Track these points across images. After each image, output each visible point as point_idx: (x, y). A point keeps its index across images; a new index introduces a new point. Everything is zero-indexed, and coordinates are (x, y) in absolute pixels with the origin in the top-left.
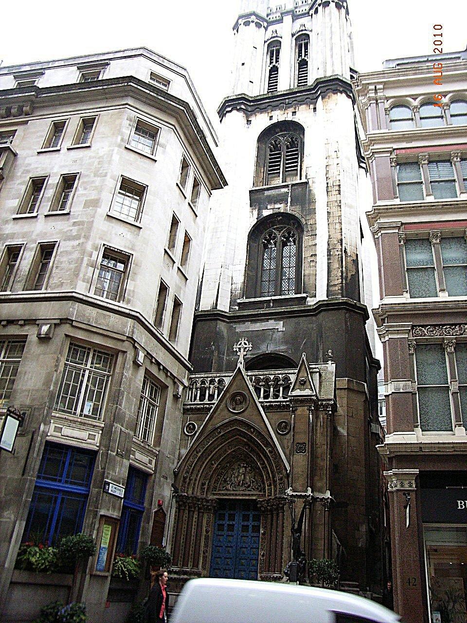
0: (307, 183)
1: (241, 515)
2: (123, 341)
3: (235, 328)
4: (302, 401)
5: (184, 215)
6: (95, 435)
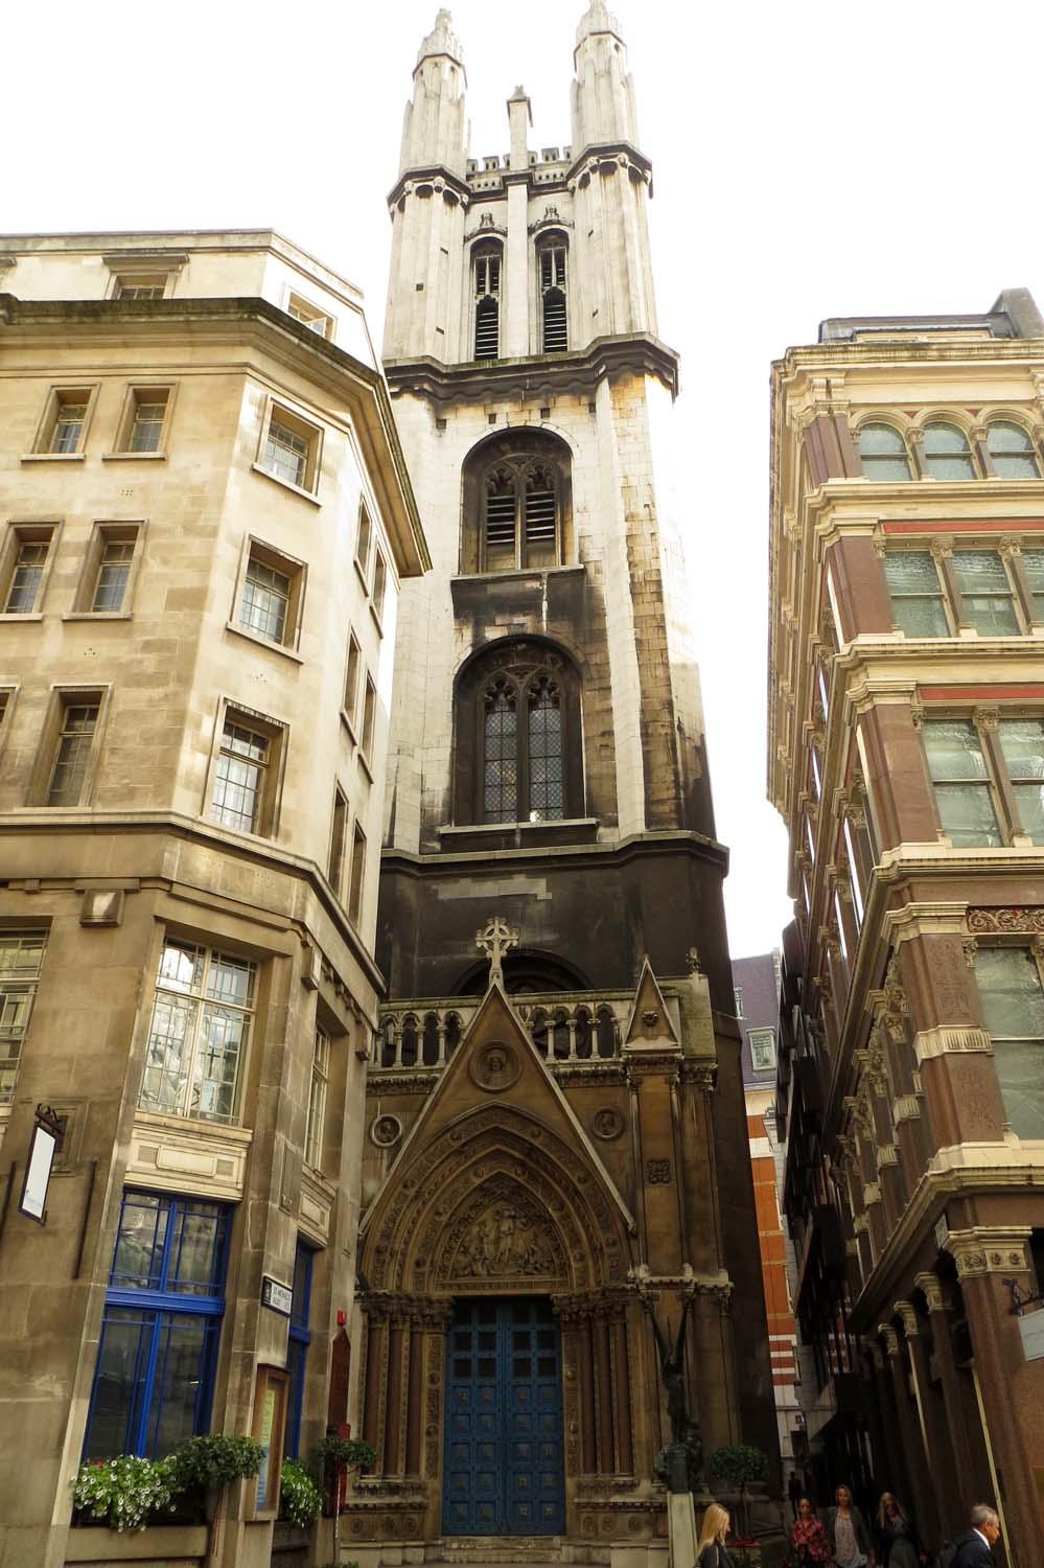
0: (582, 573)
2: (282, 930)
3: (436, 892)
4: (651, 1063)
5: (366, 637)
6: (232, 1163)
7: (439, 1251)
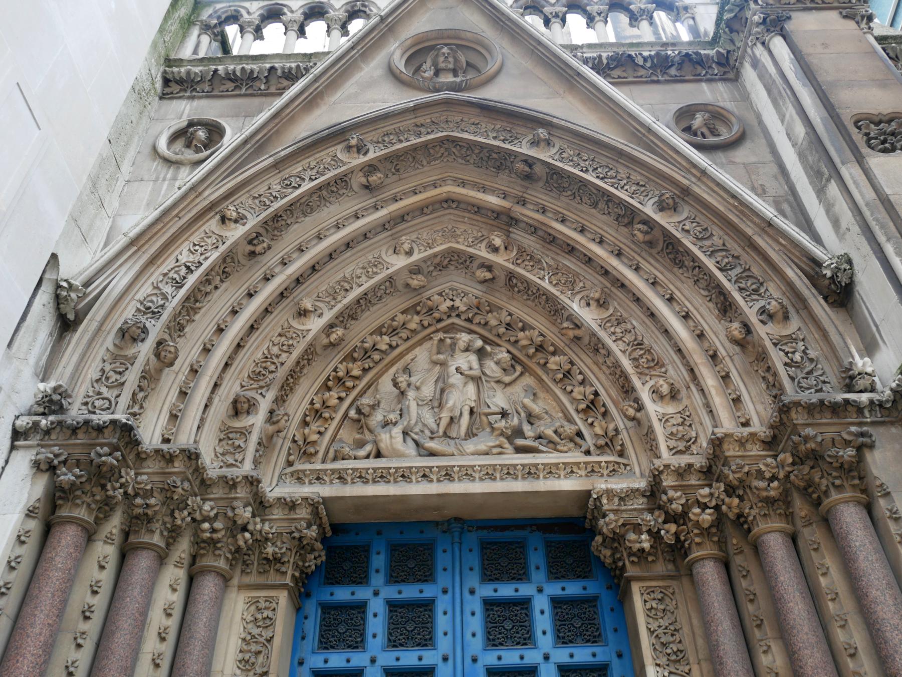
1: (475, 604)
7: (297, 405)
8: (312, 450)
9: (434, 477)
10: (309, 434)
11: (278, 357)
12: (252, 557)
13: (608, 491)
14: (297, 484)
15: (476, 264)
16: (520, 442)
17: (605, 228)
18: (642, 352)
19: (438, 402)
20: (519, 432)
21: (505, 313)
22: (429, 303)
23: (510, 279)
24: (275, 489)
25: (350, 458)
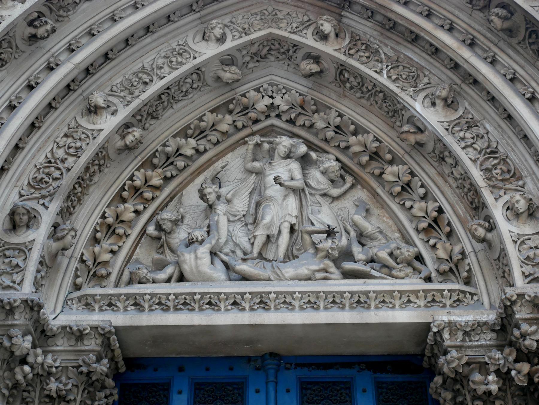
7: (86, 219)
8: (103, 272)
9: (247, 305)
10: (100, 253)
11: (63, 161)
12: (33, 394)
13: (450, 324)
14: (86, 311)
15: (300, 54)
16: (348, 266)
17: (457, 13)
18: (496, 161)
19: (253, 219)
20: (347, 255)
21: (334, 114)
22: (244, 100)
23: (341, 73)
24: (59, 315)
25: (147, 281)
